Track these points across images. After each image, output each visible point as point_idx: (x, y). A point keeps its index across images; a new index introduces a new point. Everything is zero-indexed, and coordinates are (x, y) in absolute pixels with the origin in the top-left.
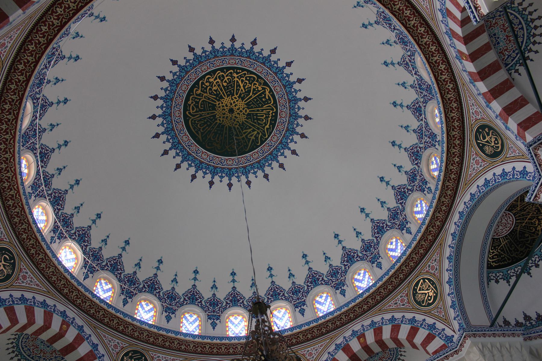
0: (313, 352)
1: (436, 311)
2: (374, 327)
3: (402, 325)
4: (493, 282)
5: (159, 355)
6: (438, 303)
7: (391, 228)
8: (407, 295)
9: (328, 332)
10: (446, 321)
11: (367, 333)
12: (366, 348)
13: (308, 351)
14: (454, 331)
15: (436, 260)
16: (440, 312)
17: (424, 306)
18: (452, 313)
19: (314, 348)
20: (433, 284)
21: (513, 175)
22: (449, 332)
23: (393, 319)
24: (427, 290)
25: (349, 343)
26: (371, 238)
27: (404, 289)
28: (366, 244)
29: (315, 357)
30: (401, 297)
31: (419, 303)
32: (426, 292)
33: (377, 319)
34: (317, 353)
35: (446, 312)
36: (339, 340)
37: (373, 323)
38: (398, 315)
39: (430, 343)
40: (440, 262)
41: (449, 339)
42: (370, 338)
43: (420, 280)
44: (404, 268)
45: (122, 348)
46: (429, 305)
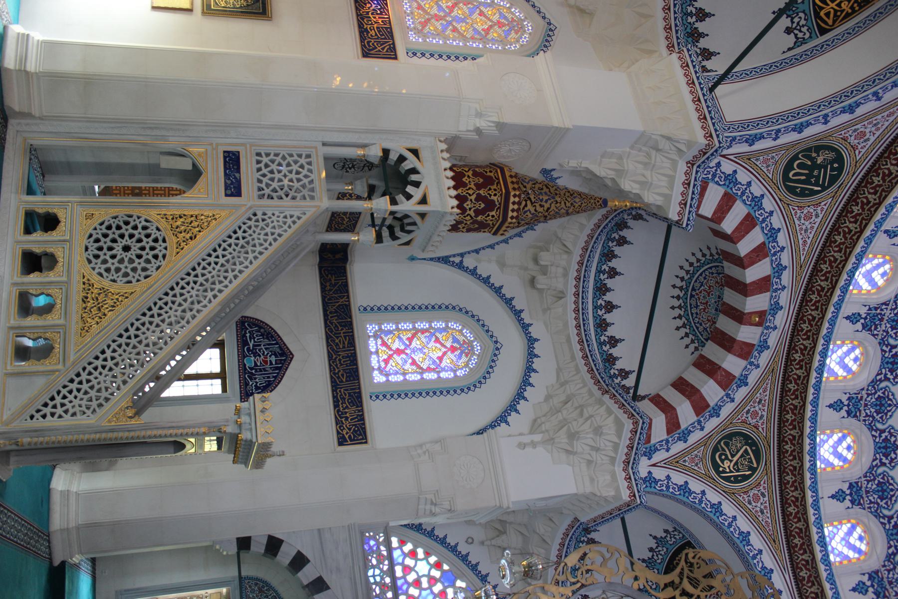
0: (807, 223)
2: (756, 347)
3: (723, 393)
6: (705, 466)
7: (872, 468)
8: (756, 427)
9: (816, 270)
10: (674, 463)
11: (759, 330)
12: (739, 317)
13: (817, 216)
14: (654, 465)
15: (762, 512)
16: (692, 460)
17: (719, 442)
18: (678, 479)
19: (812, 228)
20: (737, 480)
23: (743, 381)
24: (736, 463)
25: (768, 294)
26: (890, 422)
27: (768, 430)
28: (890, 405)
29: (797, 222)
30: (762, 416)
31: (730, 436)
32: (735, 459)
33: (764, 358)
35: (686, 470)
36: (786, 278)
37: (764, 346)
38: (741, 394)
39: (667, 423)
40: (753, 518)
41: (649, 454)
43: (758, 463)
44: (794, 463)
46: (715, 450)
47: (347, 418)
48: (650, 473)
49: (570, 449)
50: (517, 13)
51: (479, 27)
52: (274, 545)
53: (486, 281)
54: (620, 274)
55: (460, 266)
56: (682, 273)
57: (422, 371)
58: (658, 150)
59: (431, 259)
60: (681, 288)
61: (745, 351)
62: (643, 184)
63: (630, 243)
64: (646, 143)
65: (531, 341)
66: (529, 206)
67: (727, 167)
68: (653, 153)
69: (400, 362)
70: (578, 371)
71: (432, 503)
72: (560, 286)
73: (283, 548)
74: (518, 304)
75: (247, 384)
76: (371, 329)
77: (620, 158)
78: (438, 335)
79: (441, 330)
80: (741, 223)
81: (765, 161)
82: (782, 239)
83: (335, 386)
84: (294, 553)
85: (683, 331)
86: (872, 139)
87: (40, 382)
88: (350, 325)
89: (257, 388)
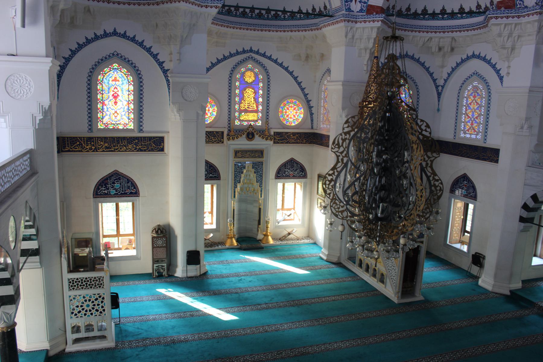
47: (491, 157)
49: (510, 49)
52: (525, 207)
53: (449, 75)
54: (444, 7)
55: (443, 87)
57: (480, 115)
58: (353, 36)
59: (439, 101)
62: (369, 39)
63: (425, 7)
64: (351, 42)
65: (474, 56)
66: (371, 96)
68: (355, 37)
69: (476, 124)
70: (485, 33)
71: (522, 128)
72: (450, 40)
73: (528, 203)
74: (459, 61)
75: (471, 196)
76: (462, 135)
77: (361, 49)
78: (468, 103)
79: (467, 100)
83: (478, 158)
84: (531, 199)
87: (388, 280)
88: (459, 145)
89: (473, 192)
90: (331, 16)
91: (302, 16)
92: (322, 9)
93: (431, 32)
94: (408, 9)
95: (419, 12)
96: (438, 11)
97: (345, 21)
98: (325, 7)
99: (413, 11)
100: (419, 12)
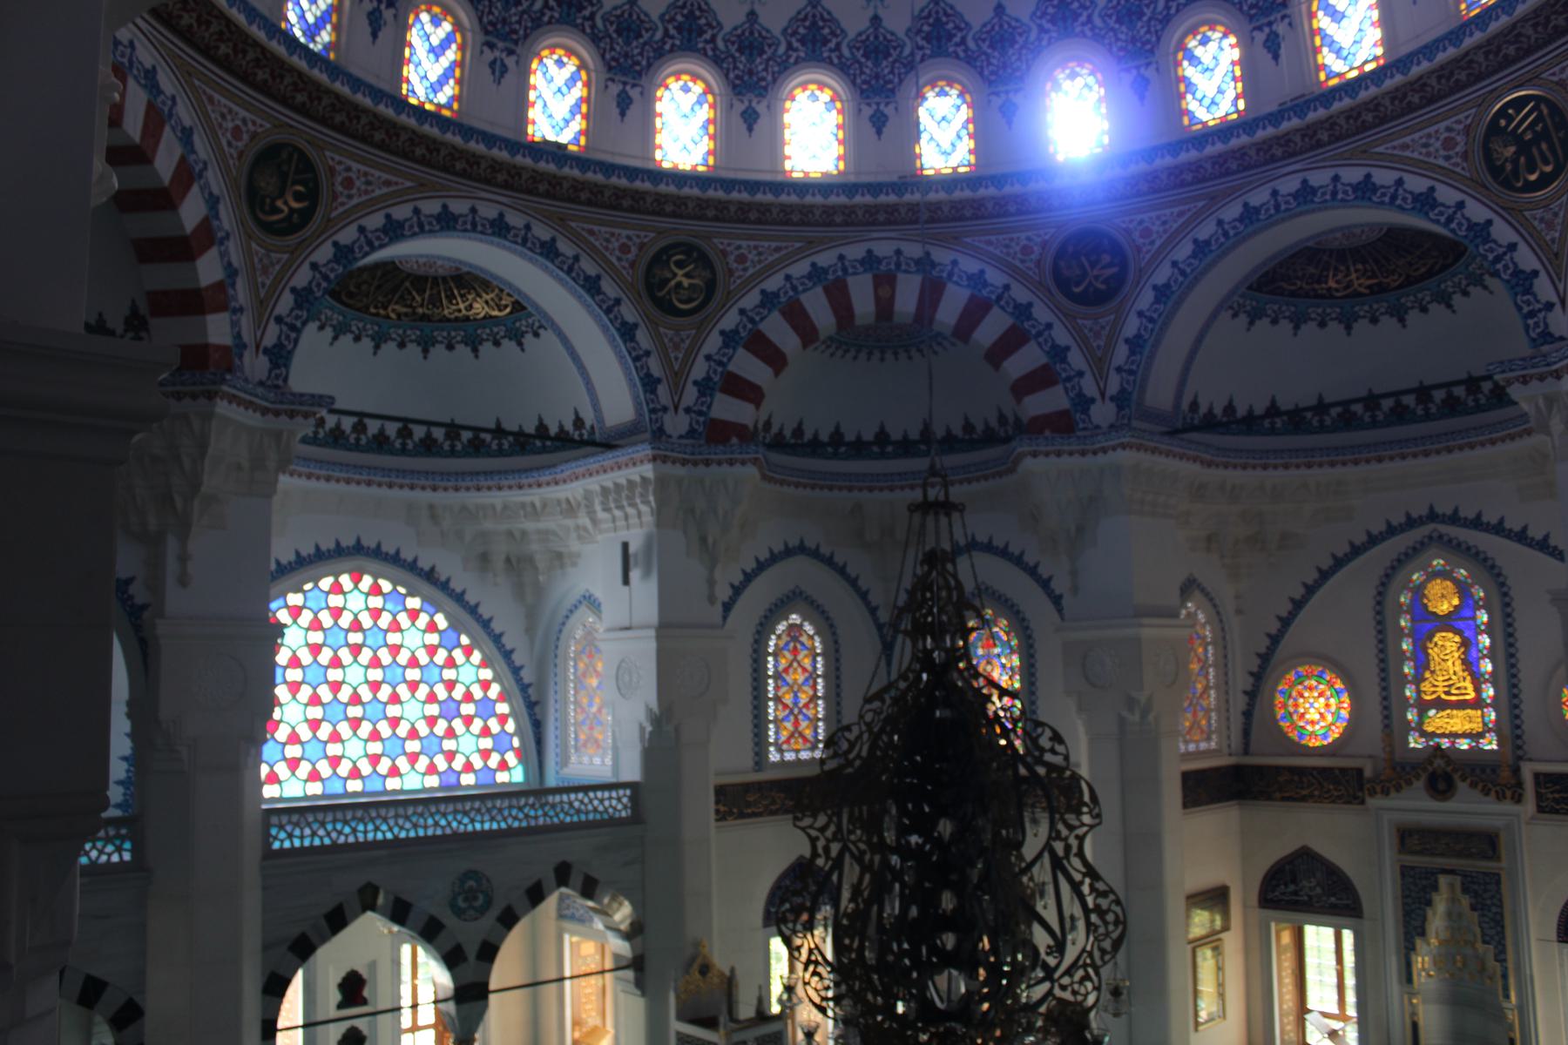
1: (1088, 323)
4: (1230, 312)
5: (349, 163)
10: (1099, 363)
12: (885, 308)
13: (739, 247)
14: (1103, 395)
18: (1121, 354)
21: (1498, 259)
22: (1089, 387)
29: (751, 271)
30: (1029, 239)
34: (760, 262)
36: (825, 259)
41: (1083, 403)
42: (907, 298)
45: (254, 136)
48: (1112, 399)
50: (579, 633)
51: (594, 682)
56: (863, 355)
60: (883, 352)
61: (932, 292)
67: (690, 395)
80: (756, 354)
81: (676, 347)
82: (774, 283)
85: (936, 348)
86: (625, 233)
90: (608, 446)
91: (506, 446)
92: (569, 427)
93: (860, 489)
94: (798, 432)
95: (824, 437)
96: (868, 436)
97: (654, 459)
98: (579, 422)
99: (808, 436)
100: (824, 437)
